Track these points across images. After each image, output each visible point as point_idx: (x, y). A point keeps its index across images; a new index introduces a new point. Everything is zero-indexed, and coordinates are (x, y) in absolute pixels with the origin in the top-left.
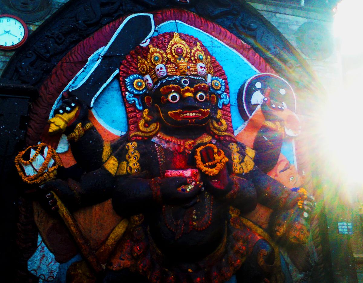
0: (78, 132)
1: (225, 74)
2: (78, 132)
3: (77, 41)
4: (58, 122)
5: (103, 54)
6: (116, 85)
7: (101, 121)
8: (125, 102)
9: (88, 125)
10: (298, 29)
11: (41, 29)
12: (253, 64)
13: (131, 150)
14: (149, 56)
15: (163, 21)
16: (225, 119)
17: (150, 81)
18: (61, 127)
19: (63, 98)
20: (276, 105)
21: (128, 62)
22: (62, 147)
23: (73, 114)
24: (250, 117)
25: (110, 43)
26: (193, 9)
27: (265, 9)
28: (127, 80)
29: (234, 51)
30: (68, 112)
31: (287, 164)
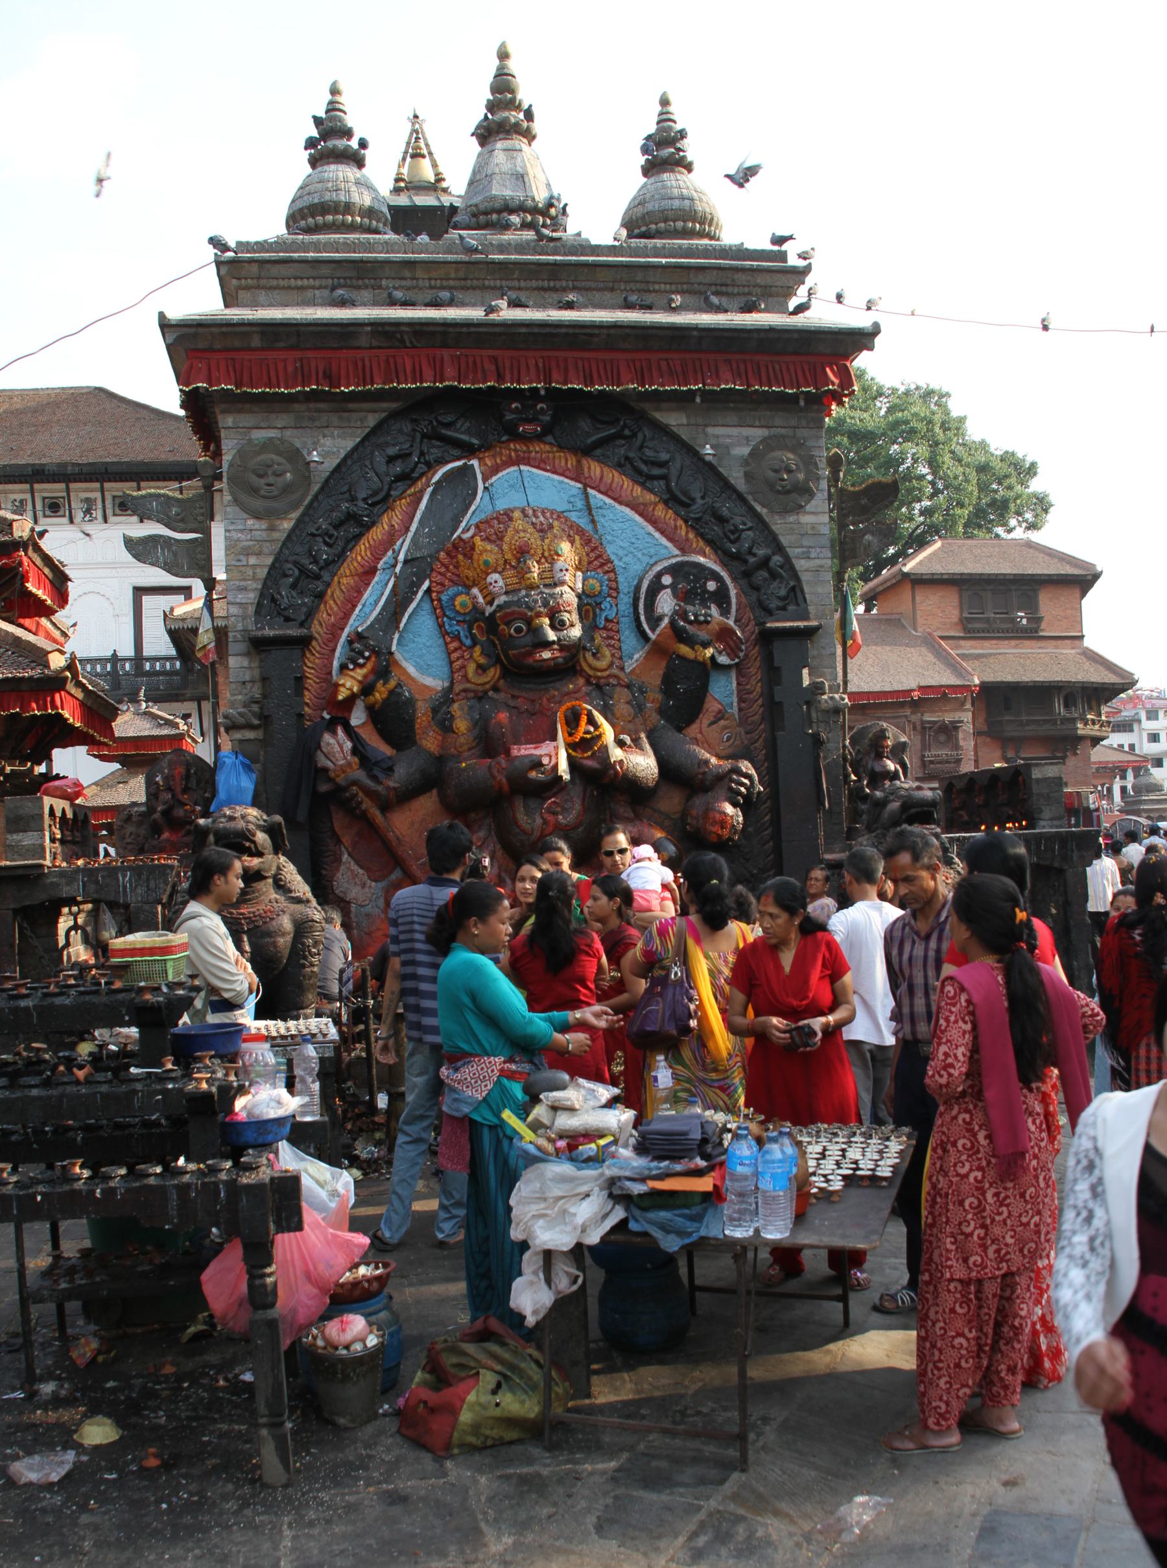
0: (379, 695)
1: (609, 561)
2: (379, 695)
3: (358, 537)
4: (349, 684)
5: (401, 557)
6: (427, 606)
7: (411, 670)
8: (444, 633)
9: (392, 683)
10: (751, 454)
11: (300, 521)
12: (662, 533)
13: (458, 714)
14: (475, 557)
15: (496, 470)
16: (609, 646)
17: (481, 600)
18: (355, 689)
19: (350, 642)
20: (696, 616)
21: (443, 565)
22: (358, 718)
23: (369, 665)
24: (653, 636)
25: (410, 535)
26: (549, 438)
27: (685, 421)
28: (444, 598)
29: (627, 510)
30: (362, 666)
31: (720, 712)
